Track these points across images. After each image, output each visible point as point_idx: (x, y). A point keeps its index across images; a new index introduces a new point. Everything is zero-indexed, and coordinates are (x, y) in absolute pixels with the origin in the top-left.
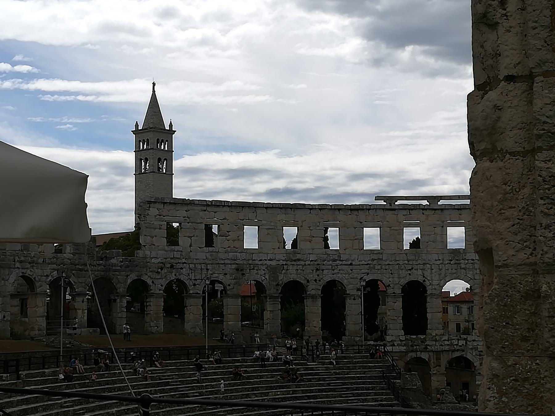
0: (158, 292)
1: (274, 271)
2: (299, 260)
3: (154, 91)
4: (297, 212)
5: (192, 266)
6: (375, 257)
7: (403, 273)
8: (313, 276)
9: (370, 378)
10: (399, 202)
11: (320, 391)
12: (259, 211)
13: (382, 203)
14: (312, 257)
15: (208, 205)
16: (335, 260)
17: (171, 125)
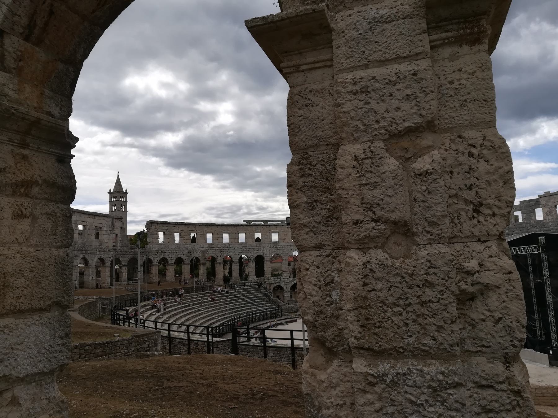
0: (156, 263)
1: (204, 252)
2: (213, 248)
3: (118, 175)
4: (212, 227)
5: (170, 251)
6: (243, 245)
7: (255, 252)
8: (219, 254)
9: (260, 297)
10: (252, 223)
11: (245, 304)
12: (197, 227)
13: (245, 223)
14: (219, 246)
15: (176, 224)
16: (228, 247)
17: (126, 190)
